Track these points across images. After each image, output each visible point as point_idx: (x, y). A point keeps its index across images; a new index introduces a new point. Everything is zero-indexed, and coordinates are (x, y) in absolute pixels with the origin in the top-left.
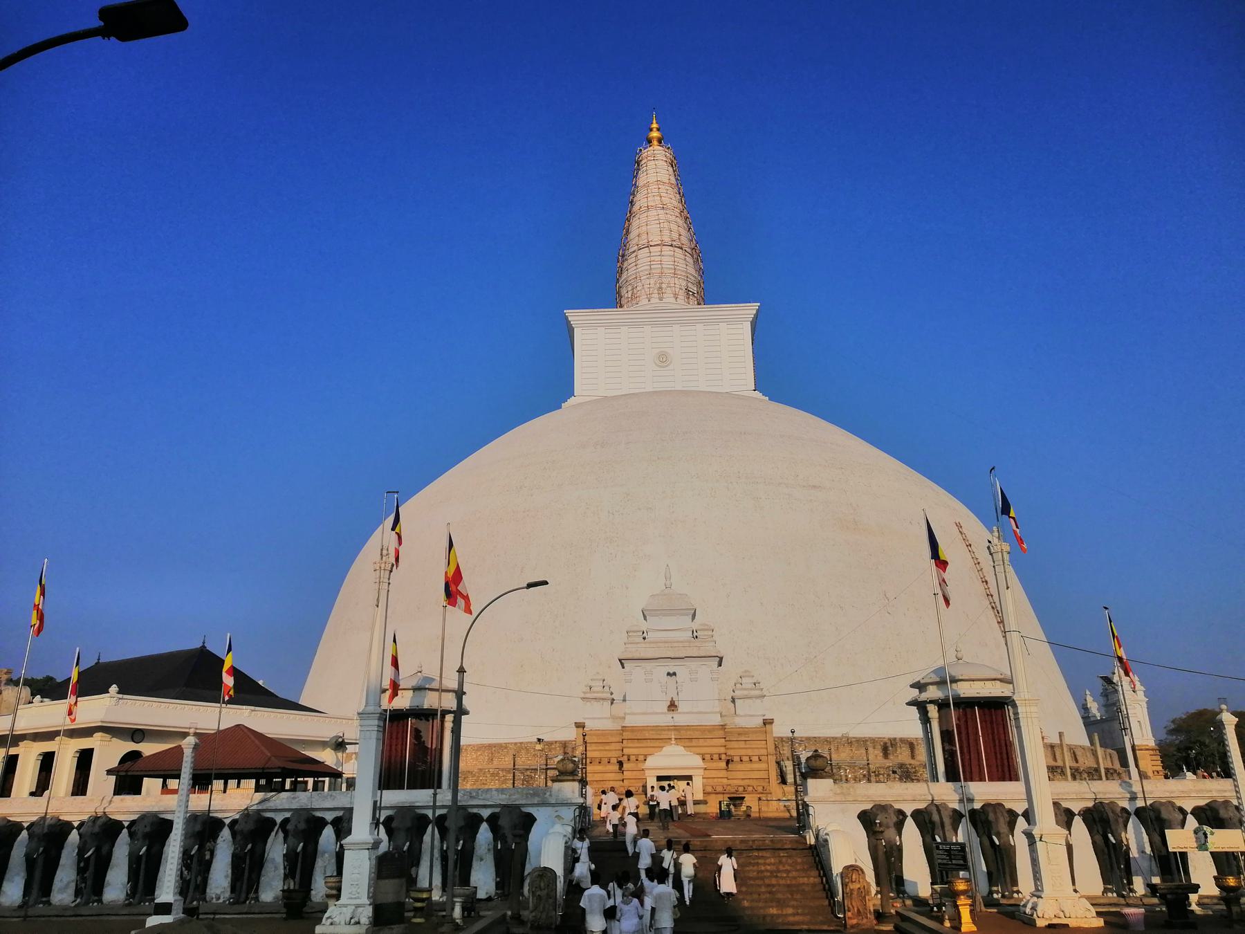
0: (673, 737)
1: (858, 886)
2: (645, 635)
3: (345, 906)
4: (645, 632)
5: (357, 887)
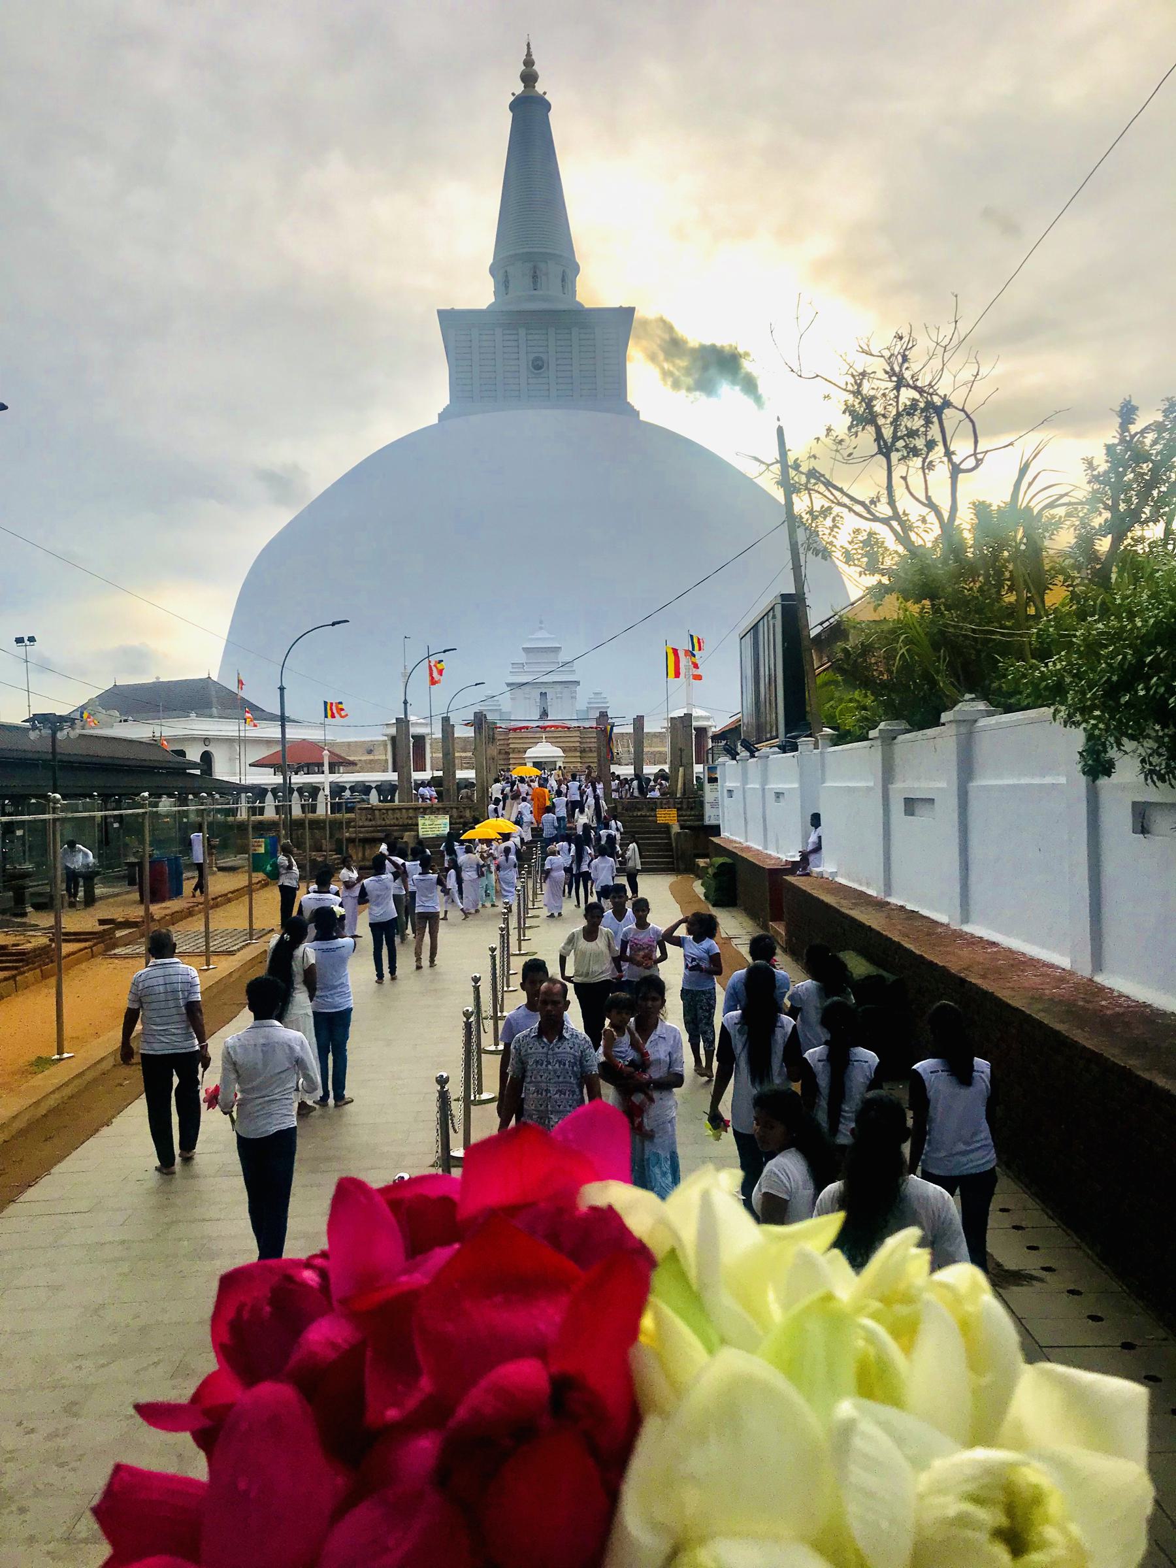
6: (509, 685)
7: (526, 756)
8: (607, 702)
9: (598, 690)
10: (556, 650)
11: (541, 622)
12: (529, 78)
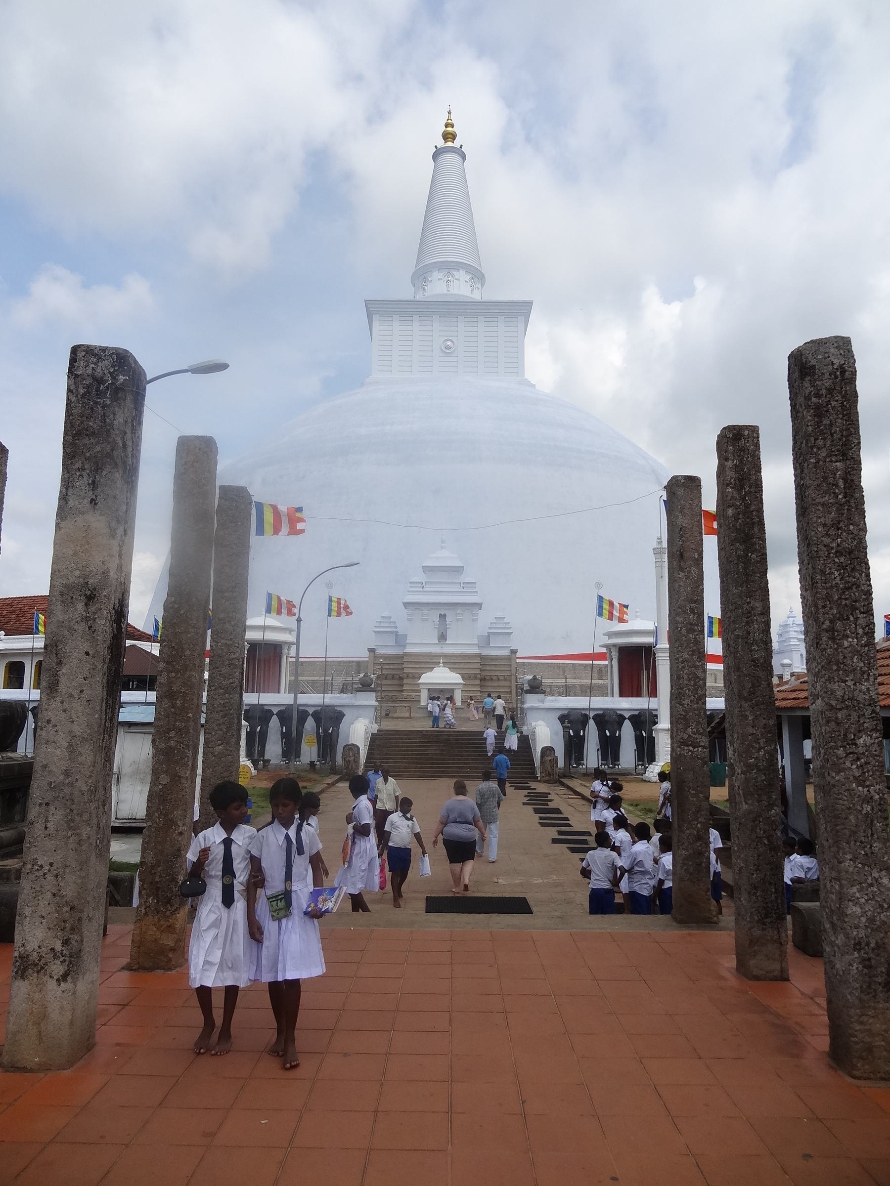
0: (441, 661)
1: (550, 758)
2: (424, 584)
4: (424, 583)
6: (407, 605)
7: (420, 681)
8: (510, 628)
9: (500, 615)
10: (458, 570)
11: (443, 542)
12: (449, 136)
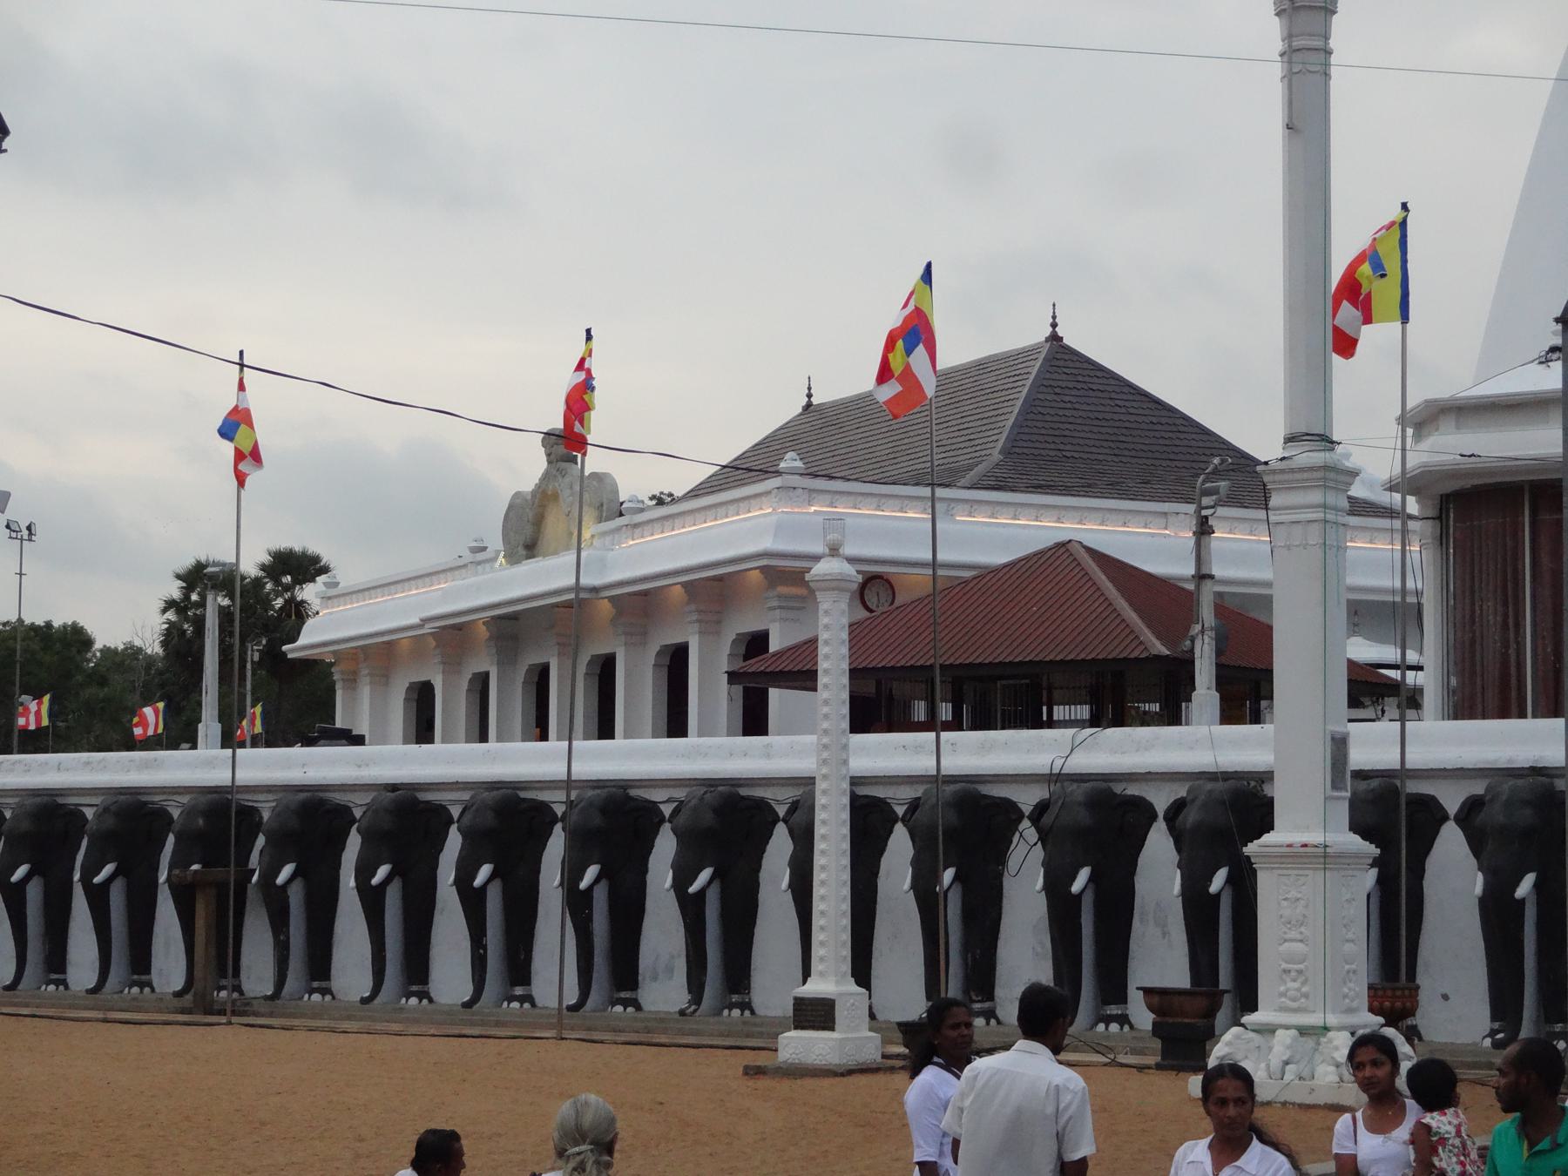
3: (1268, 1030)
5: (1302, 979)
